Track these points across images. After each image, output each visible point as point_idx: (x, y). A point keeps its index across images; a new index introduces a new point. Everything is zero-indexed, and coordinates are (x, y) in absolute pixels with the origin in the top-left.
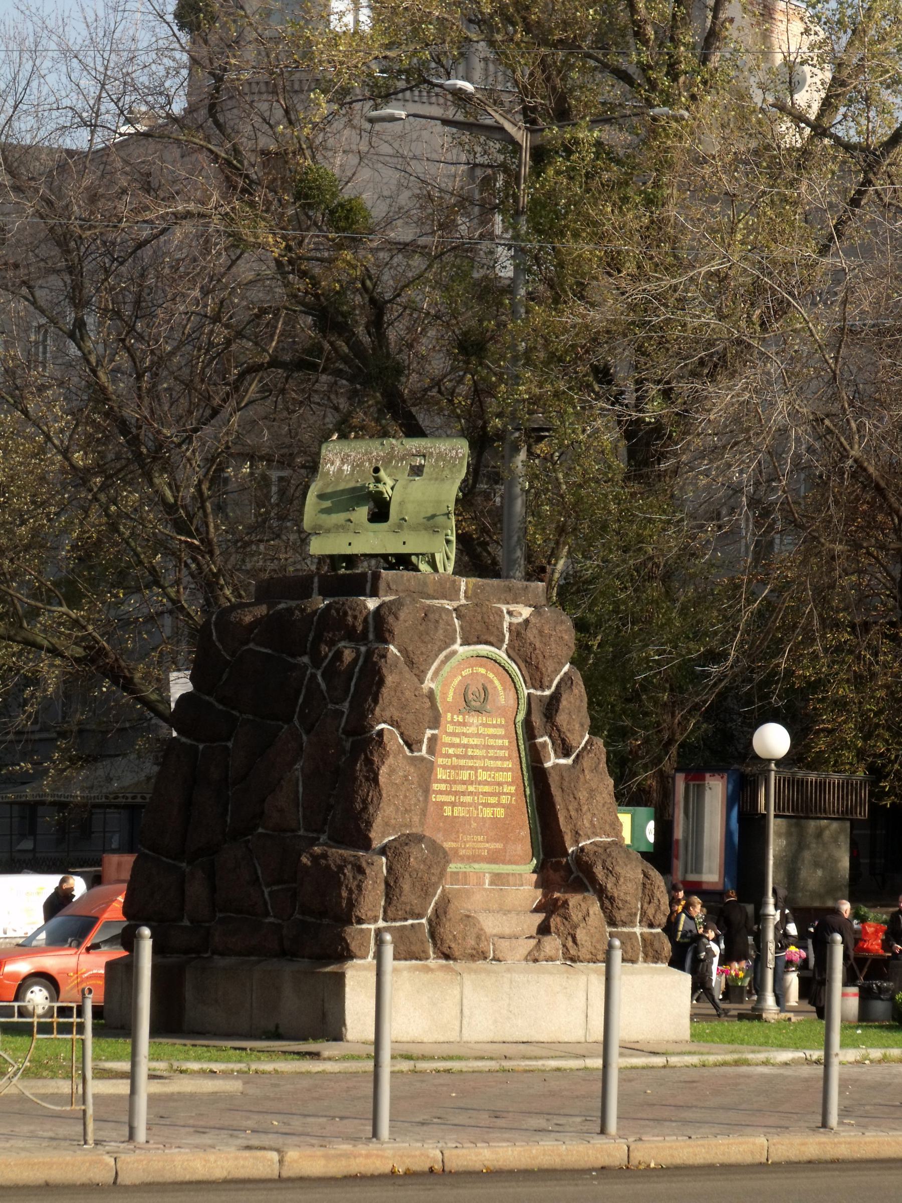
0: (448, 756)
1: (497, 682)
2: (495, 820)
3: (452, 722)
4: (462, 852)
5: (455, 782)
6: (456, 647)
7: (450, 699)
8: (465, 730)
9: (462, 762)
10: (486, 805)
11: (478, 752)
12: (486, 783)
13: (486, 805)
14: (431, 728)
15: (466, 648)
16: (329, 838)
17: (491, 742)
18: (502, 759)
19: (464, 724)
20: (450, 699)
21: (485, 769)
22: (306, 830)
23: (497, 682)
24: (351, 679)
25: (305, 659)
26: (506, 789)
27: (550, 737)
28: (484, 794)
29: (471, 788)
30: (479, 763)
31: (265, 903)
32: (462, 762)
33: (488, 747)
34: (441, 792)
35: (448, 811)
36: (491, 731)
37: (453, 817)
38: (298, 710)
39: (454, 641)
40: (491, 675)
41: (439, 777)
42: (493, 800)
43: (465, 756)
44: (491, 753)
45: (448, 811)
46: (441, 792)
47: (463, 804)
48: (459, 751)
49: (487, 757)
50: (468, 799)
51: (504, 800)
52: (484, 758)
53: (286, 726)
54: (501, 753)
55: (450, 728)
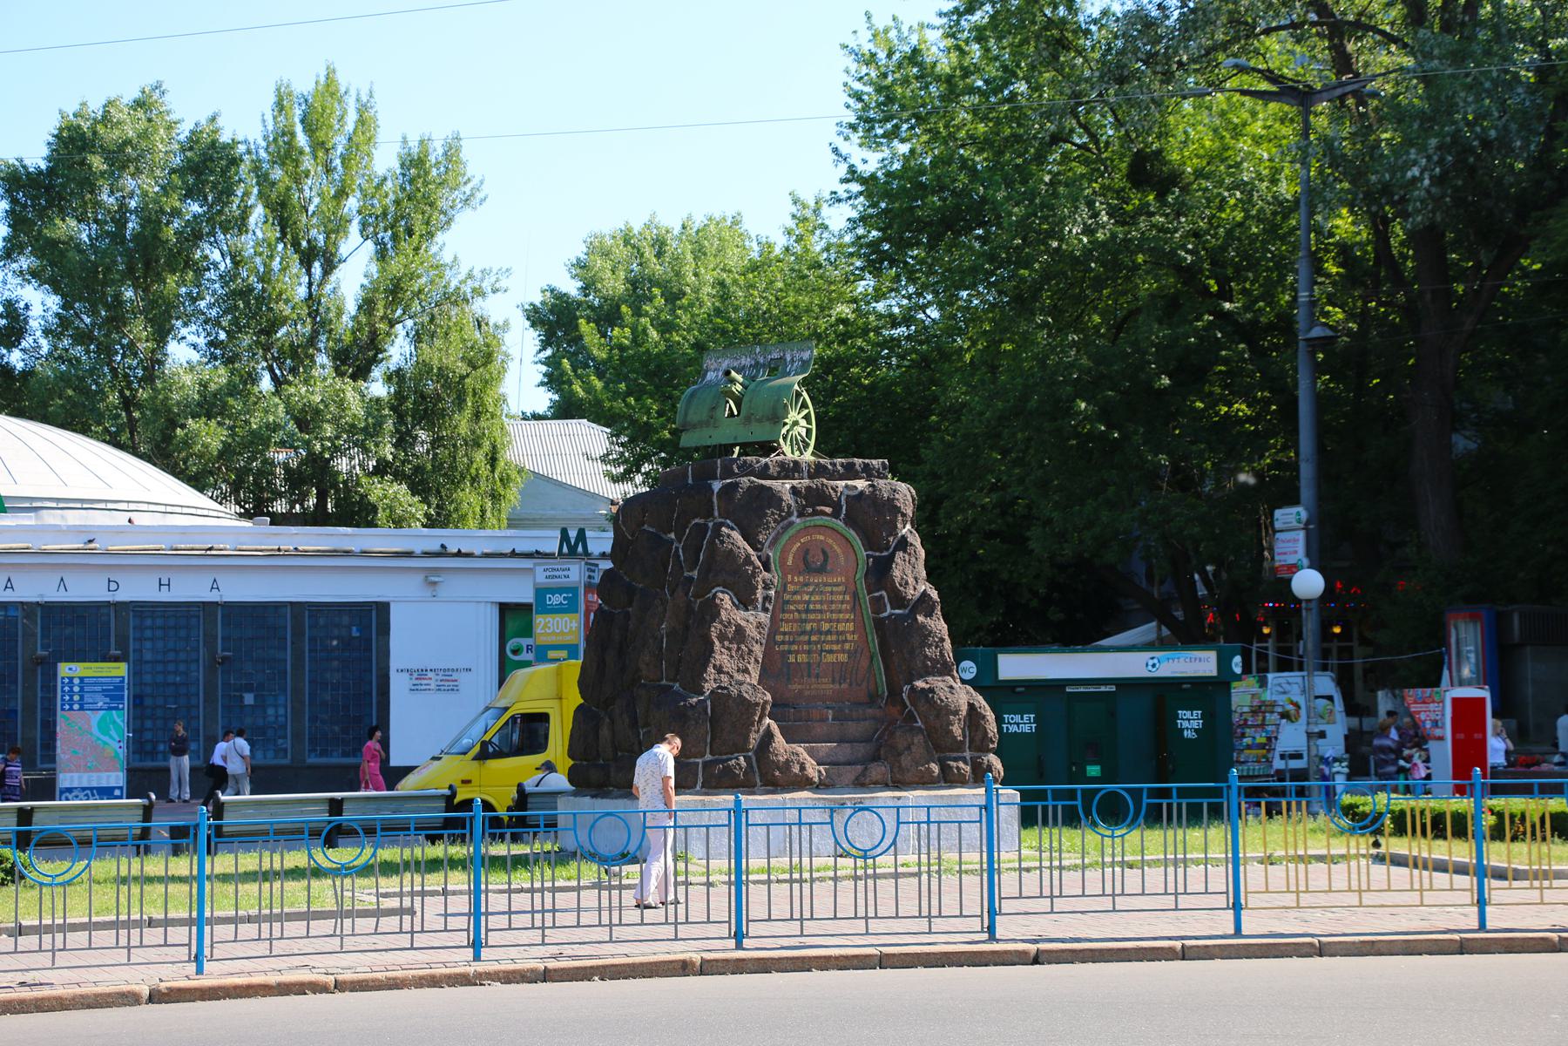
3: (792, 582)
6: (794, 518)
7: (790, 563)
10: (830, 652)
11: (818, 607)
12: (829, 632)
13: (830, 652)
18: (846, 611)
20: (790, 563)
21: (831, 621)
25: (672, 536)
26: (849, 637)
29: (814, 638)
34: (783, 643)
35: (792, 659)
42: (835, 647)
43: (807, 611)
45: (792, 659)
46: (783, 643)
51: (847, 646)
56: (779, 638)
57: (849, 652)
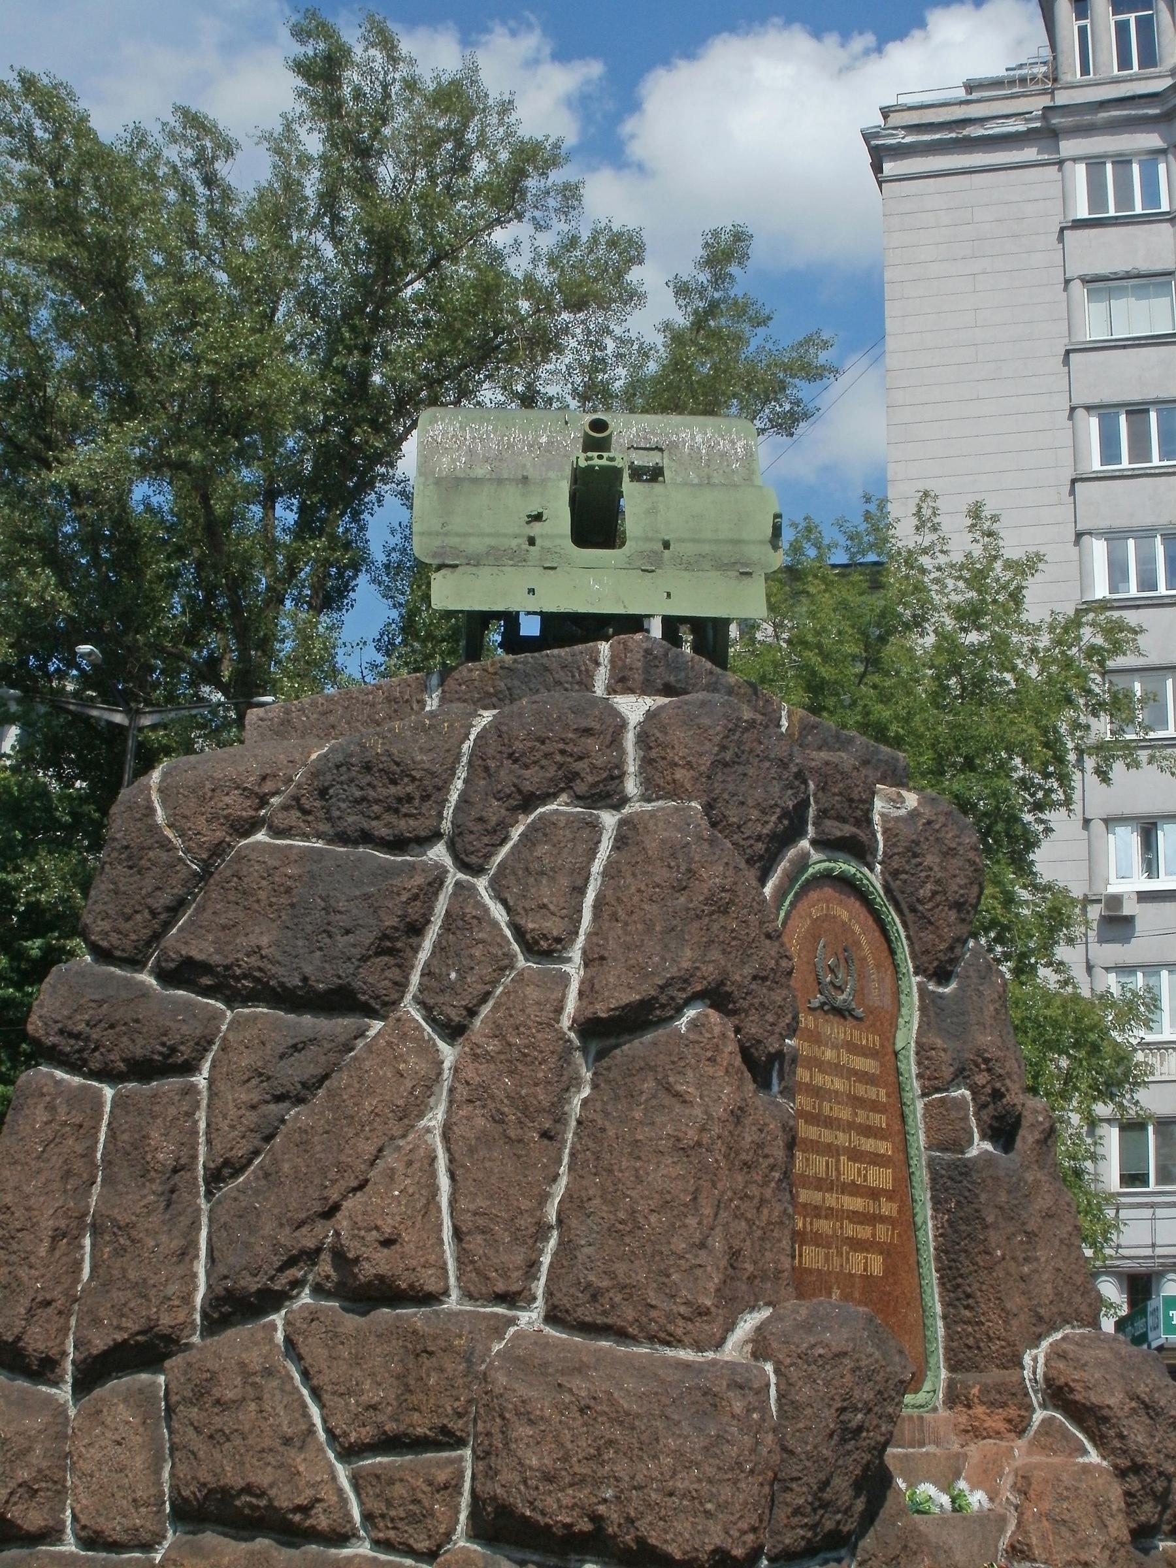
6: (805, 844)
16: (552, 1317)
22: (468, 1295)
24: (581, 891)
25: (439, 853)
27: (970, 1088)
31: (344, 1501)
38: (415, 979)
39: (802, 833)
53: (377, 1025)
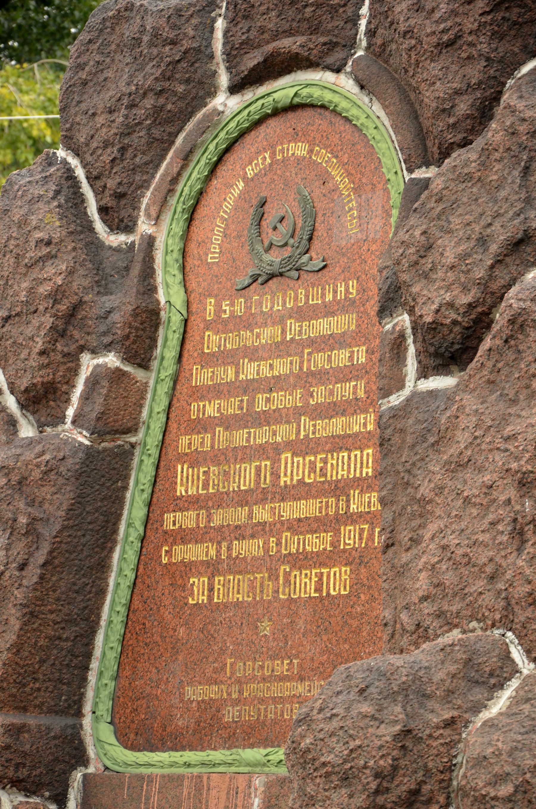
0: (203, 425)
1: (337, 175)
2: (323, 602)
4: (230, 714)
5: (220, 500)
8: (248, 338)
9: (240, 438)
10: (302, 560)
11: (282, 400)
12: (301, 491)
13: (302, 560)
14: (94, 352)
15: (249, 95)
17: (320, 361)
19: (247, 322)
21: (302, 447)
23: (337, 175)
28: (299, 526)
29: (262, 514)
30: (283, 433)
32: (240, 438)
33: (308, 379)
36: (323, 326)
37: (212, 607)
40: (322, 156)
41: (180, 490)
42: (316, 543)
44: (320, 395)
45: (198, 589)
46: (183, 536)
47: (238, 566)
48: (232, 407)
49: (305, 410)
50: (250, 548)
51: (350, 537)
52: (298, 412)
54: (345, 390)
55: (212, 341)
56: (171, 520)
57: (355, 559)
